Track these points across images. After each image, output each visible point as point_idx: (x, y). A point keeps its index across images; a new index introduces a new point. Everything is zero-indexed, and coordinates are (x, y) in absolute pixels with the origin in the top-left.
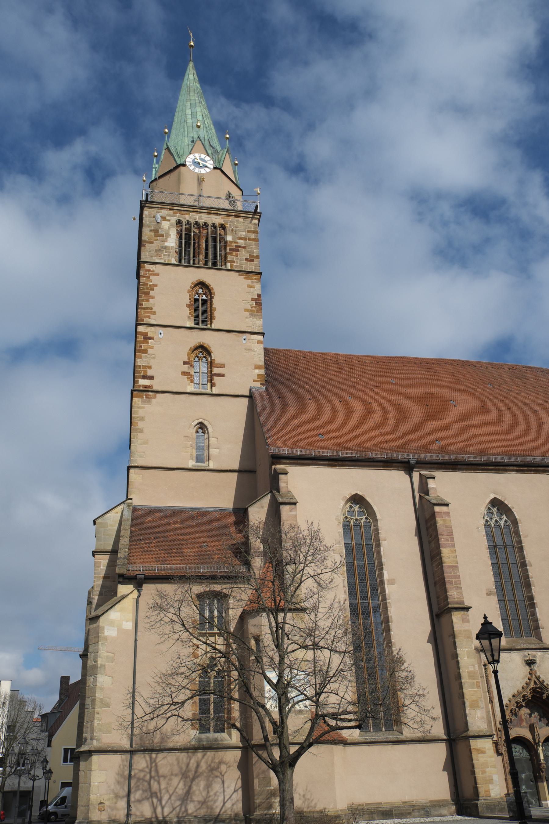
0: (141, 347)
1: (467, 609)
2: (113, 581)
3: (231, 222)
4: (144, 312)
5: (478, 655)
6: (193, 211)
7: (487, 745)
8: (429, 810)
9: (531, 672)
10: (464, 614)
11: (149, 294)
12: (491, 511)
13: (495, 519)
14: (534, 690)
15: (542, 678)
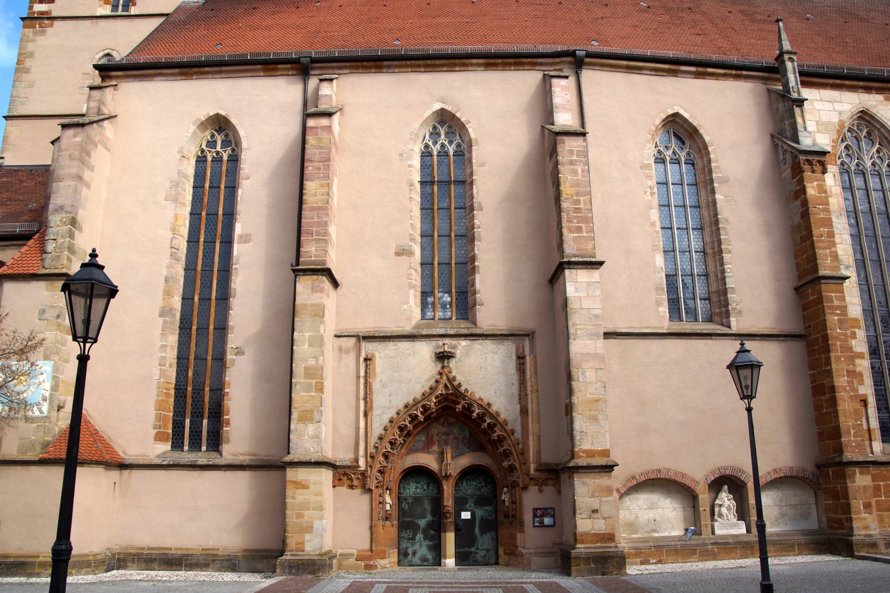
5: (358, 344)
8: (237, 562)
9: (441, 371)
10: (318, 279)
13: (441, 142)
15: (459, 378)
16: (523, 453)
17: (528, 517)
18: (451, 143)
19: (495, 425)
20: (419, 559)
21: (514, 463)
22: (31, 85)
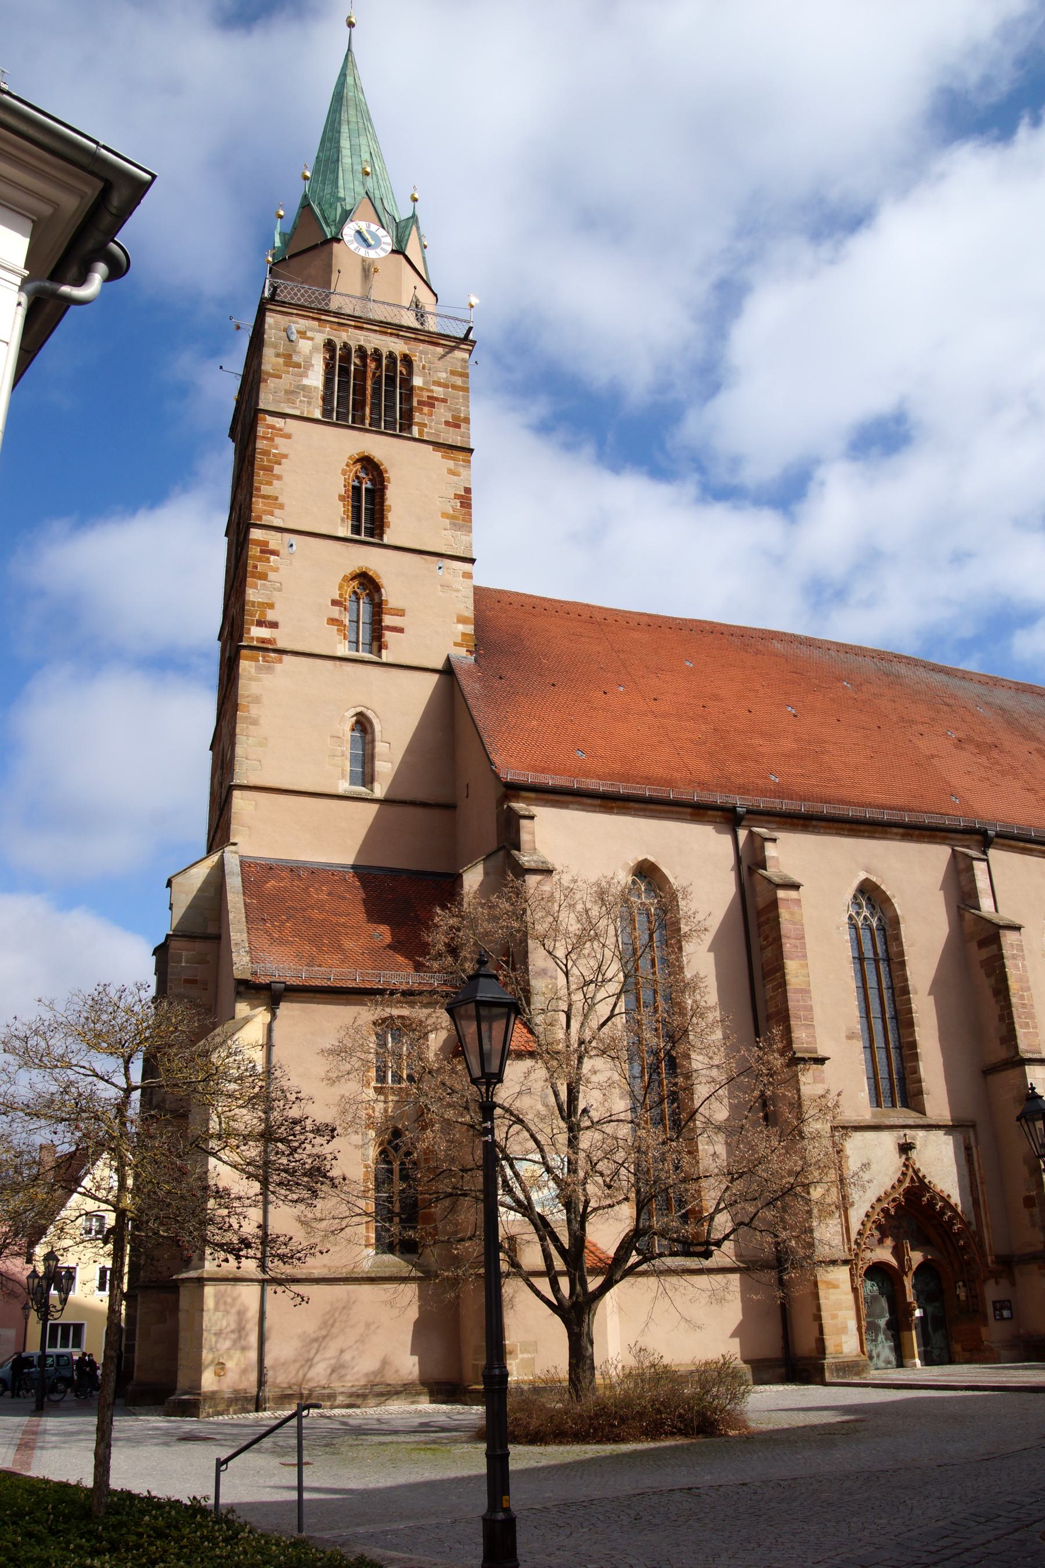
0: (256, 567)
1: (821, 1061)
2: (204, 989)
3: (421, 352)
4: (262, 502)
6: (356, 327)
7: (842, 1274)
9: (907, 1163)
10: (818, 1068)
11: (272, 471)
12: (859, 901)
14: (908, 1192)
16: (981, 1245)
17: (990, 1310)
18: (872, 915)
20: (884, 1362)
22: (263, 743)
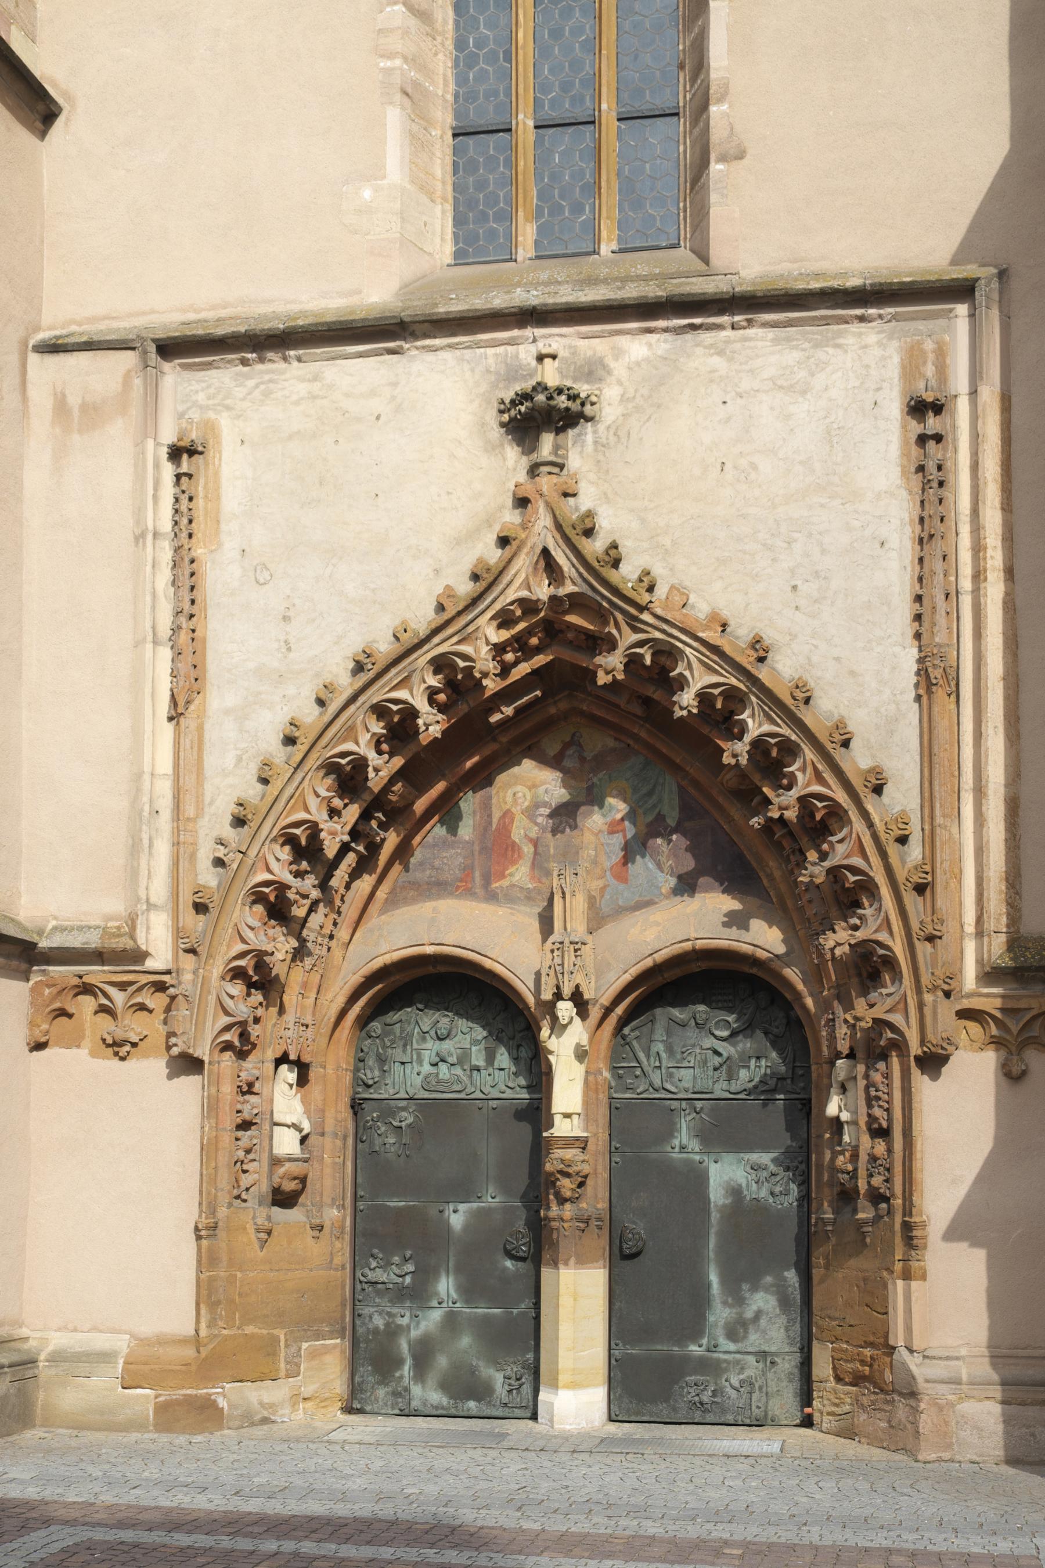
9: (528, 491)
19: (789, 750)
21: (883, 937)
